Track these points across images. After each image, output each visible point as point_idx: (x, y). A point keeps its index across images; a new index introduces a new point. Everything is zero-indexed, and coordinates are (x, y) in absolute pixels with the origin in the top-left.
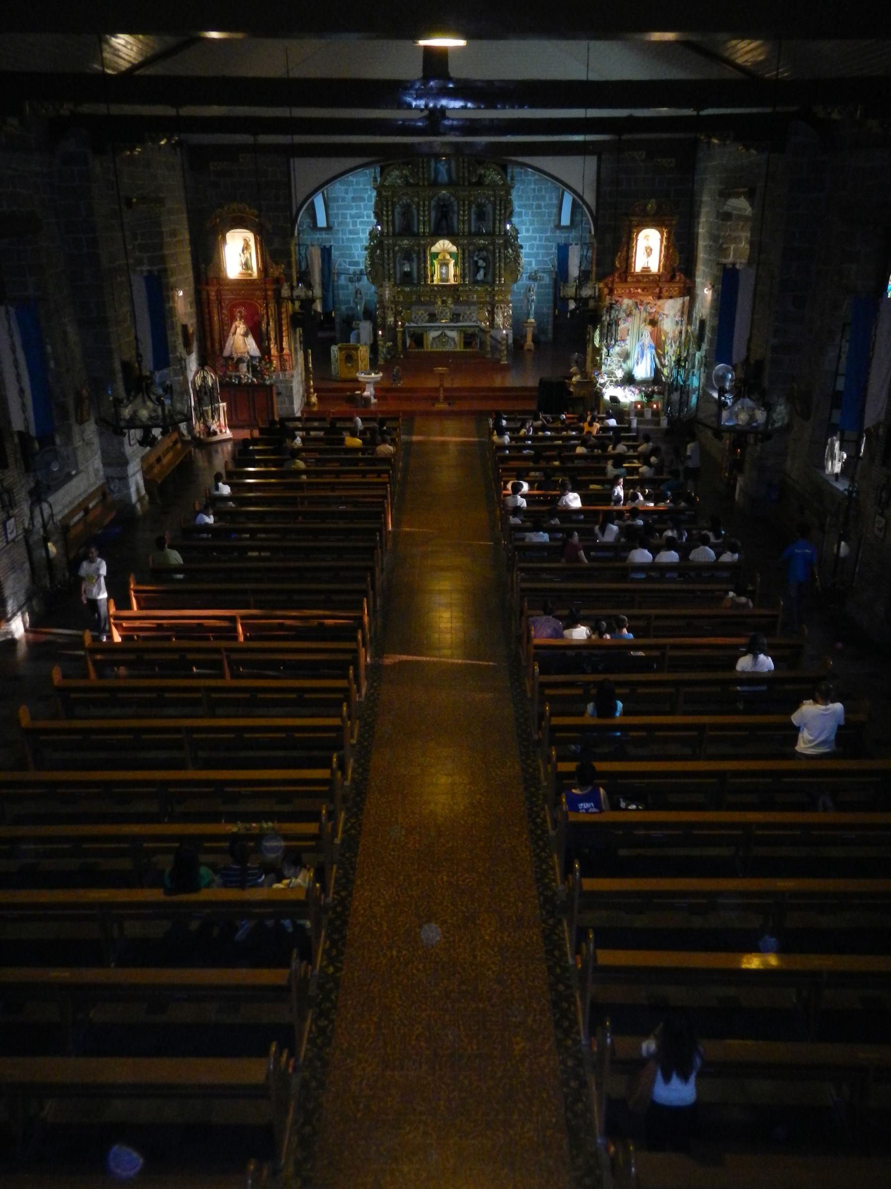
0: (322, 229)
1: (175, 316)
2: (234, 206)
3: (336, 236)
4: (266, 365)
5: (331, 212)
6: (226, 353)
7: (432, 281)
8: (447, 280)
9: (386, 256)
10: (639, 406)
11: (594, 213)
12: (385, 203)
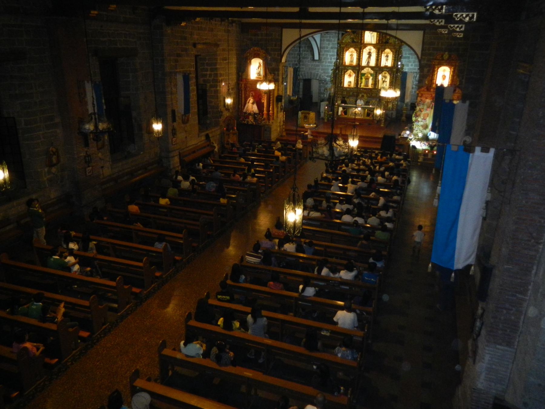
0: (316, 60)
1: (220, 93)
2: (256, 48)
3: (323, 64)
4: (260, 117)
5: (321, 53)
6: (244, 111)
7: (361, 86)
8: (368, 86)
9: (340, 73)
10: (427, 152)
11: (420, 58)
12: (342, 50)
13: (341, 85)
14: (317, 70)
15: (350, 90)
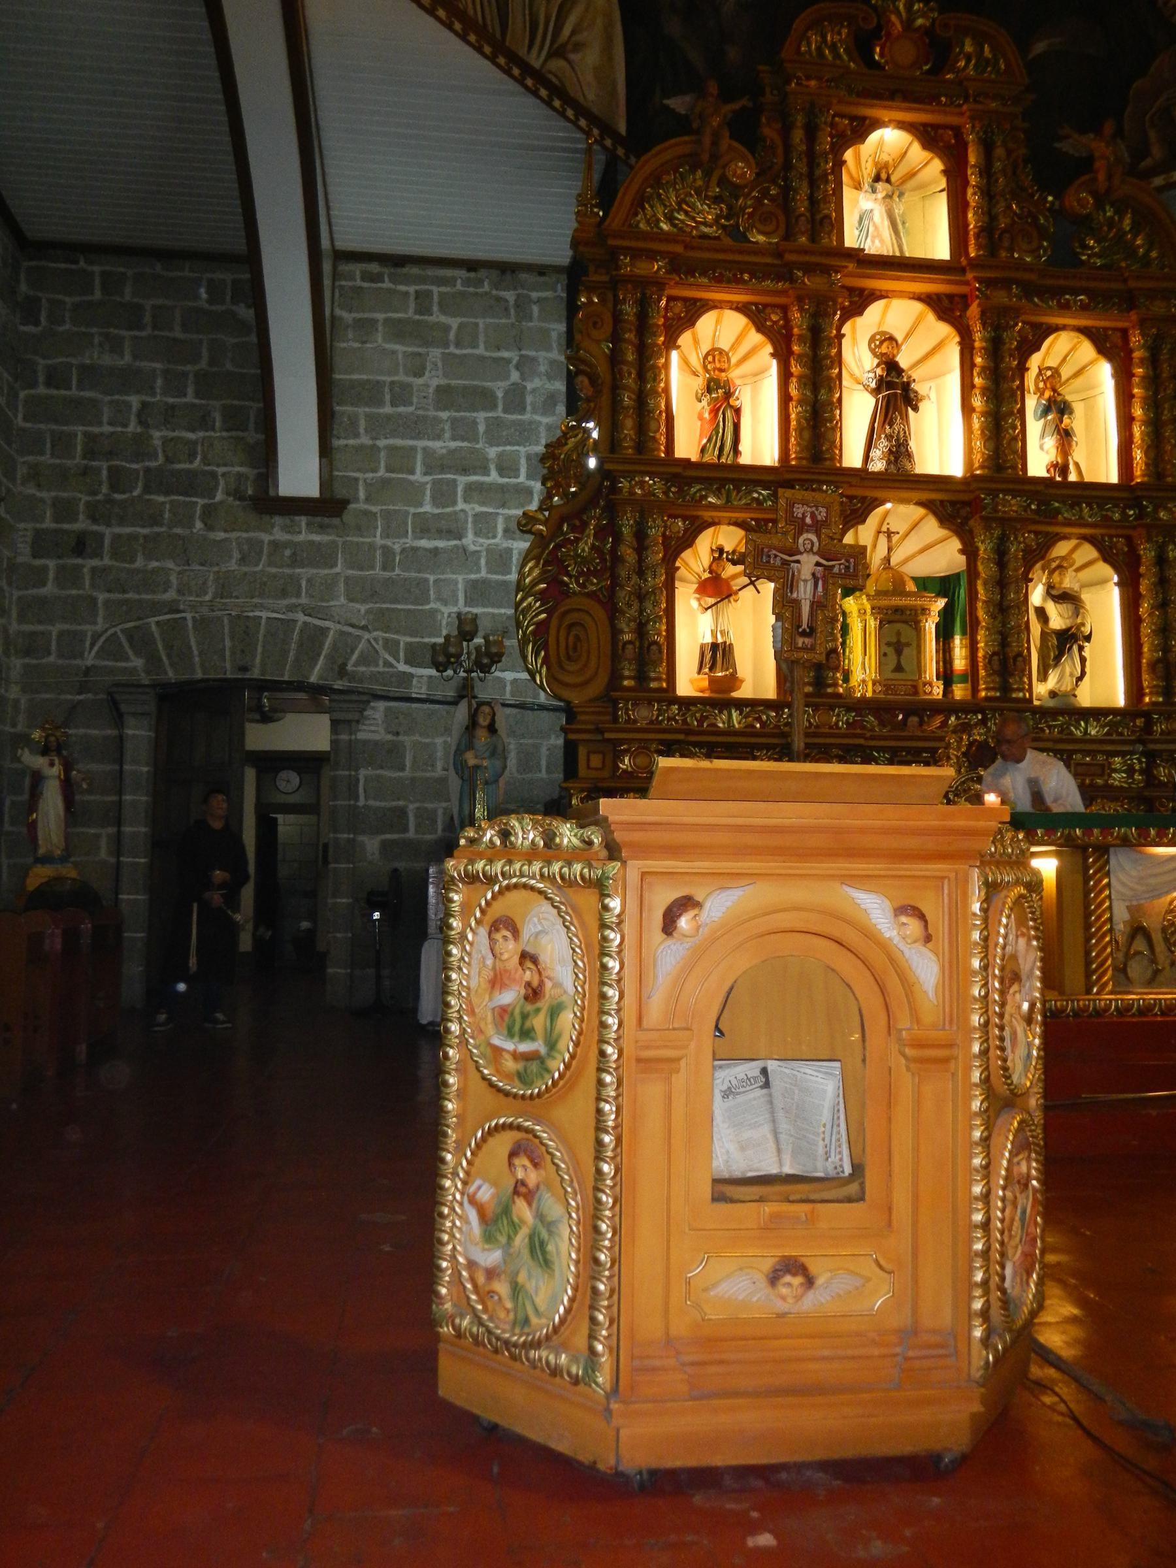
9: (628, 553)
12: (629, 310)
13: (642, 677)
14: (304, 600)
15: (748, 731)
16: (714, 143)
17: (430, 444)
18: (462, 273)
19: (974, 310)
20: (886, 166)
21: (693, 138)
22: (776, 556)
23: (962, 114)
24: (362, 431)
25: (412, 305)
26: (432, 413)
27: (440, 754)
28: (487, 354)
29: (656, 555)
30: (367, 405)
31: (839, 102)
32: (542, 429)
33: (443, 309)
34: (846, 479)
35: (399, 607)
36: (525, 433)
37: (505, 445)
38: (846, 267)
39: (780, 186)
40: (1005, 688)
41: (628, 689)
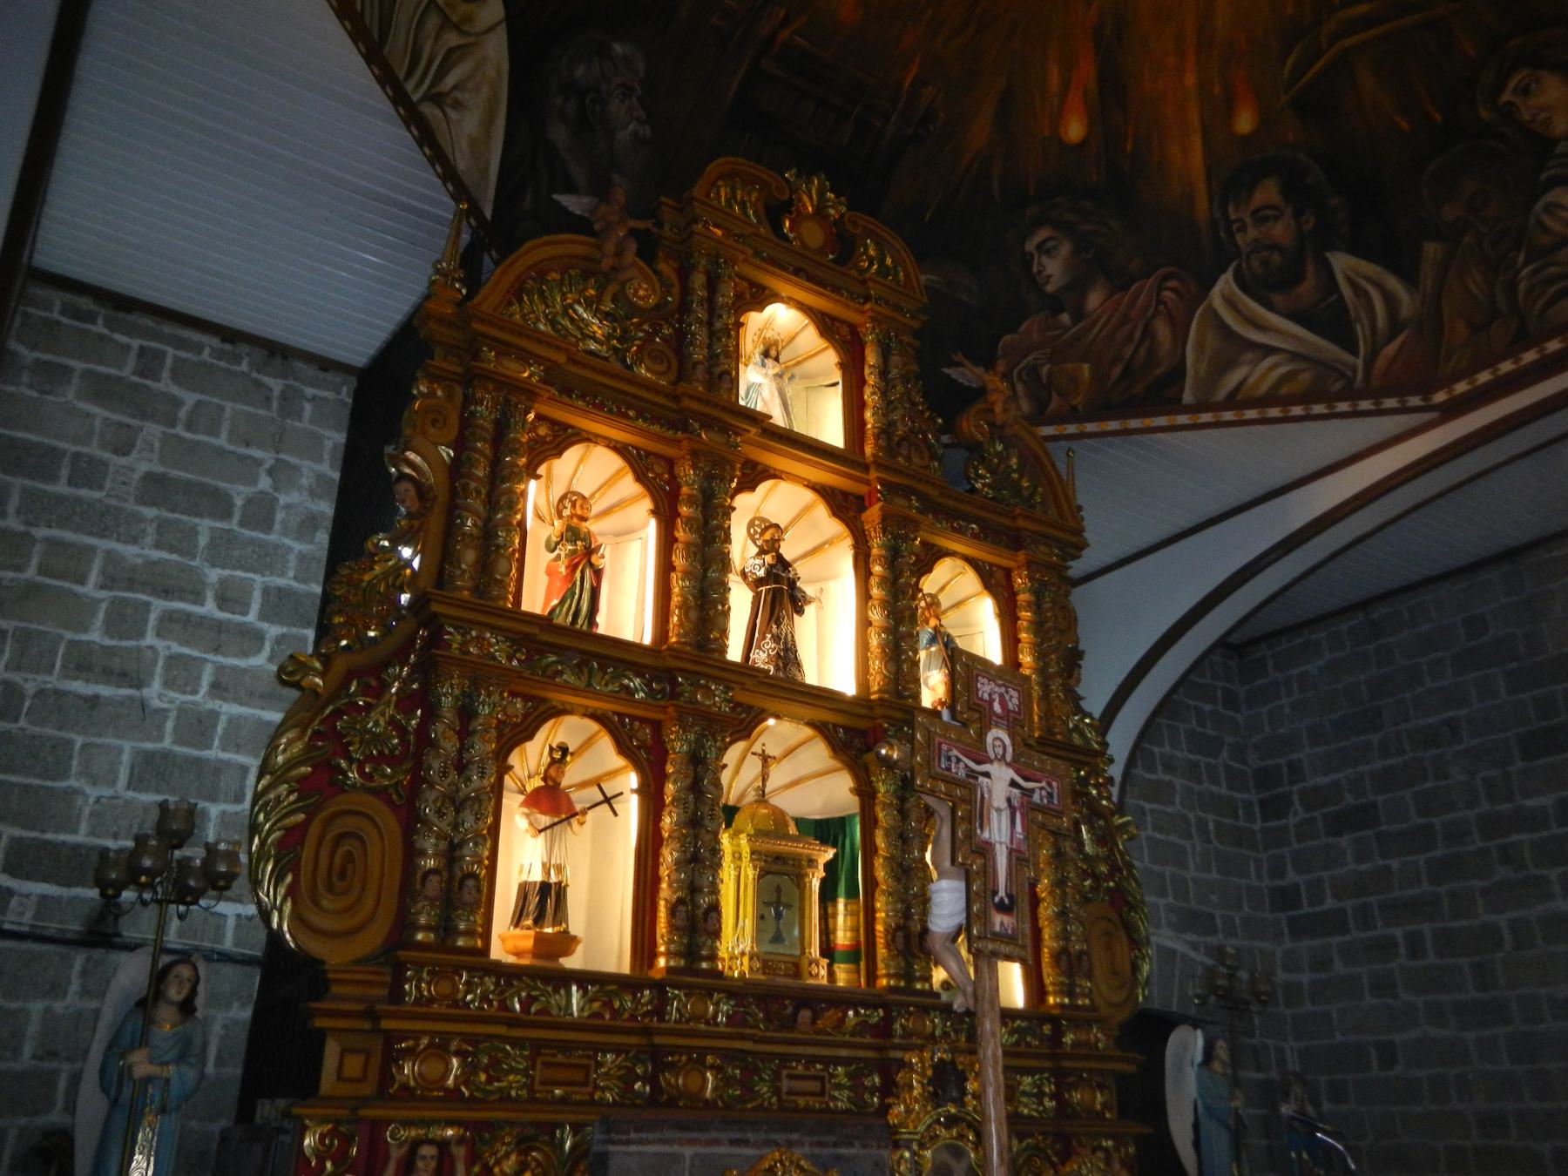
13: (446, 928)
16: (619, 254)
17: (119, 547)
18: (215, 342)
19: (873, 514)
20: (776, 343)
21: (592, 240)
22: (959, 760)
23: (864, 312)
24: (11, 509)
25: (131, 362)
26: (130, 506)
27: (32, 1030)
28: (231, 448)
29: (483, 747)
30: (30, 476)
31: (745, 261)
32: (292, 558)
33: (178, 375)
34: (741, 679)
35: (14, 779)
36: (268, 559)
37: (234, 568)
38: (749, 431)
39: (674, 327)
40: (909, 976)
41: (422, 946)
